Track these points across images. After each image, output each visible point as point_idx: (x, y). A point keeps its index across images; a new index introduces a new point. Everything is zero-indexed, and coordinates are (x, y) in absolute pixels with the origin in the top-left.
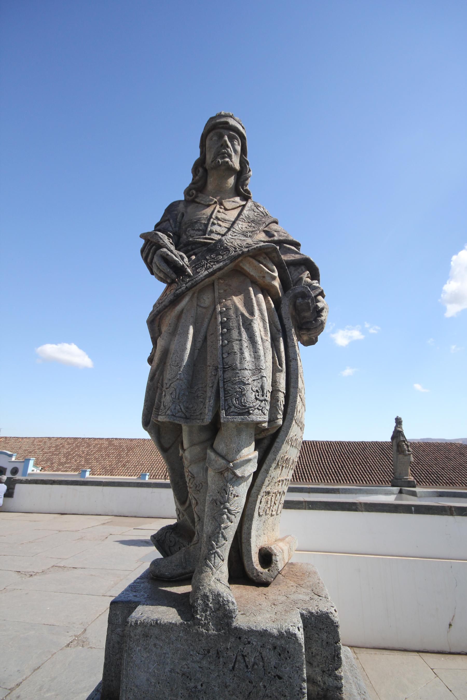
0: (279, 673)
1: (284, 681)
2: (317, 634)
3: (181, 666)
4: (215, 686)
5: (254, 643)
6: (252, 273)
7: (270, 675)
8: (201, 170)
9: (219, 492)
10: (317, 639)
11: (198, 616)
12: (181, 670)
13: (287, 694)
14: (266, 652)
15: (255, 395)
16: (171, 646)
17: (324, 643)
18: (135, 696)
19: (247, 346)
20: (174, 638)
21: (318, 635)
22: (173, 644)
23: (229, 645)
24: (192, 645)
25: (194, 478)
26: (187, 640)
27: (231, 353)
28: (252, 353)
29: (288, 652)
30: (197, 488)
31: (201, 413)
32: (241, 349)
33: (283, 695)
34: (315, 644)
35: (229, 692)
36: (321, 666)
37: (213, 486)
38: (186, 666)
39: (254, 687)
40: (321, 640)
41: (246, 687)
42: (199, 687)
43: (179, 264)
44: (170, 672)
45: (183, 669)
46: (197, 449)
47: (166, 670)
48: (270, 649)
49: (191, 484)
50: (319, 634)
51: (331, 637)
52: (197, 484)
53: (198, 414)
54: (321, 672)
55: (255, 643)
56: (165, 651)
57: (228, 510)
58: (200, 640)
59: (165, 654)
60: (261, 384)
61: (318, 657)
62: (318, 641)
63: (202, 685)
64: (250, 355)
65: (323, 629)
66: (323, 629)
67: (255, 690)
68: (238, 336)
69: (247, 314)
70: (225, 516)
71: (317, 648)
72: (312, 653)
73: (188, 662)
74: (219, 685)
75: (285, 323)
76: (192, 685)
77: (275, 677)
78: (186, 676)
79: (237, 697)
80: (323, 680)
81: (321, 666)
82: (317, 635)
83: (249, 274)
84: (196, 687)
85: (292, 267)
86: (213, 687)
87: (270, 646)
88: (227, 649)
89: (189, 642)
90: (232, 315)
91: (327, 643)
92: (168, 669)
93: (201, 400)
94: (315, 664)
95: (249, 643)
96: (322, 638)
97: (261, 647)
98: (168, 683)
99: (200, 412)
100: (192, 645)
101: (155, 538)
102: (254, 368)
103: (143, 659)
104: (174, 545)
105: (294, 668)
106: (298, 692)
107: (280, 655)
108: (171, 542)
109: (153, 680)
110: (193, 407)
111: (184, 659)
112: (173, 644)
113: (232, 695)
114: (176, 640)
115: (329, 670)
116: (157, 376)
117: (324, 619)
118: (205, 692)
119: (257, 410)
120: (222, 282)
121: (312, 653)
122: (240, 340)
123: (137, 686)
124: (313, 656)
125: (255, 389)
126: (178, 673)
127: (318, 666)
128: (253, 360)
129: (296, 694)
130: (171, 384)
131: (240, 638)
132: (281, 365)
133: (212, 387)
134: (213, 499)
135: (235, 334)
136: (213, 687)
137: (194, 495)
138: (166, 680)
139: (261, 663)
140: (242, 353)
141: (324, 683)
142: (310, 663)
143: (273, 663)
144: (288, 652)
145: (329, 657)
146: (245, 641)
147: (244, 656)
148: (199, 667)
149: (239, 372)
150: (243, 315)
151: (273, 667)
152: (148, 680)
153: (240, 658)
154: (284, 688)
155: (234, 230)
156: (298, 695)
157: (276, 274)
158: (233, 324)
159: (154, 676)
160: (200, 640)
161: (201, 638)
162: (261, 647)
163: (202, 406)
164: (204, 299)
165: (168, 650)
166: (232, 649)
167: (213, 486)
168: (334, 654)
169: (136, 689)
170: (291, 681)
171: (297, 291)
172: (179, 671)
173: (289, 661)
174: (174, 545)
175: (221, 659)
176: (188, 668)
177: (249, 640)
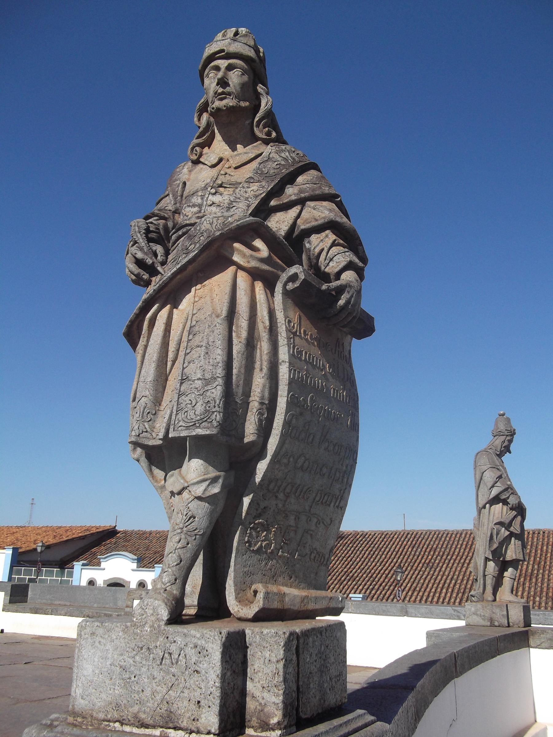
0: (198, 669)
1: (202, 675)
2: (260, 652)
3: (119, 660)
4: (145, 678)
5: (178, 642)
7: (190, 670)
10: (260, 657)
12: (119, 664)
13: (202, 687)
14: (188, 650)
16: (112, 643)
17: (267, 661)
18: (83, 684)
20: (115, 637)
21: (262, 653)
22: (113, 642)
23: (158, 643)
24: (128, 643)
26: (125, 638)
29: (207, 651)
33: (199, 687)
34: (258, 662)
35: (156, 683)
36: (261, 683)
38: (123, 660)
39: (176, 680)
40: (264, 658)
41: (170, 680)
42: (133, 678)
44: (111, 665)
45: (120, 663)
47: (108, 663)
48: (191, 648)
50: (263, 652)
51: (273, 656)
54: (262, 688)
55: (179, 643)
56: (107, 648)
58: (135, 639)
59: (107, 650)
61: (260, 674)
62: (260, 659)
63: (135, 677)
65: (267, 647)
66: (267, 647)
67: (177, 683)
71: (260, 666)
72: (254, 670)
73: (125, 657)
74: (148, 677)
76: (127, 676)
77: (194, 672)
78: (124, 669)
79: (162, 688)
80: (262, 695)
81: (261, 683)
82: (260, 653)
84: (130, 678)
86: (144, 679)
87: (192, 645)
88: (157, 647)
89: (126, 640)
91: (269, 661)
92: (108, 663)
94: (256, 680)
95: (175, 642)
96: (265, 656)
97: (185, 646)
98: (109, 674)
100: (128, 643)
103: (90, 654)
105: (211, 665)
106: (212, 686)
107: (200, 653)
109: (97, 672)
111: (122, 655)
112: (113, 642)
113: (158, 686)
114: (116, 639)
115: (269, 686)
117: (269, 638)
118: (137, 683)
121: (254, 670)
123: (84, 676)
124: (254, 673)
126: (117, 666)
127: (259, 682)
129: (210, 687)
131: (167, 638)
136: (144, 679)
138: (107, 671)
139: (184, 660)
141: (263, 698)
142: (251, 679)
143: (193, 660)
144: (207, 651)
145: (270, 674)
146: (171, 641)
147: (170, 654)
148: (134, 662)
151: (193, 663)
152: (93, 671)
153: (166, 655)
154: (200, 682)
156: (212, 687)
159: (98, 668)
160: (135, 639)
162: (185, 646)
165: (110, 646)
166: (161, 647)
168: (275, 671)
169: (84, 678)
170: (207, 676)
172: (117, 665)
173: (207, 659)
175: (151, 655)
176: (125, 662)
177: (175, 639)
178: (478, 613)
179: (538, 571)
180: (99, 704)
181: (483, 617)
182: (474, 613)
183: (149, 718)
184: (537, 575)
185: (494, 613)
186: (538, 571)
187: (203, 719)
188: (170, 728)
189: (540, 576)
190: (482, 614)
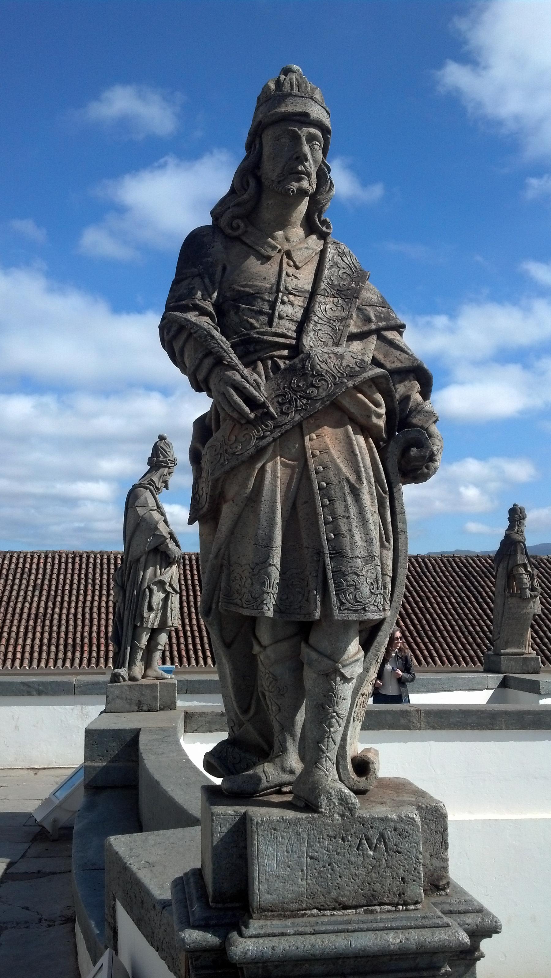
1: (404, 855)
6: (352, 410)
8: (252, 183)
9: (325, 696)
11: (323, 810)
15: (370, 589)
19: (357, 526)
25: (276, 680)
27: (338, 535)
28: (363, 536)
30: (281, 693)
31: (301, 607)
32: (350, 530)
36: (429, 851)
37: (316, 689)
43: (260, 400)
46: (284, 646)
49: (273, 687)
52: (280, 688)
53: (296, 607)
57: (337, 714)
60: (375, 575)
64: (361, 538)
68: (345, 512)
69: (352, 479)
70: (334, 720)
75: (392, 481)
83: (348, 410)
85: (396, 376)
90: (333, 478)
93: (298, 590)
99: (299, 606)
101: (214, 756)
102: (366, 554)
104: (240, 762)
108: (235, 758)
110: (287, 598)
116: (222, 550)
119: (372, 607)
120: (312, 422)
122: (348, 518)
125: (369, 581)
128: (365, 544)
130: (260, 570)
132: (388, 540)
133: (317, 576)
134: (317, 703)
135: (339, 508)
137: (276, 701)
140: (352, 536)
141: (432, 865)
149: (351, 561)
150: (348, 480)
155: (316, 319)
157: (383, 411)
158: (335, 492)
161: (327, 827)
163: (300, 598)
164: (289, 447)
167: (316, 689)
171: (410, 436)
174: (240, 762)
175: (346, 843)
178: (124, 696)
179: (53, 609)
180: (290, 896)
181: (129, 701)
182: (117, 697)
183: (351, 900)
184: (52, 615)
185: (142, 695)
186: (53, 609)
187: (409, 893)
188: (375, 905)
189: (56, 616)
190: (129, 697)
